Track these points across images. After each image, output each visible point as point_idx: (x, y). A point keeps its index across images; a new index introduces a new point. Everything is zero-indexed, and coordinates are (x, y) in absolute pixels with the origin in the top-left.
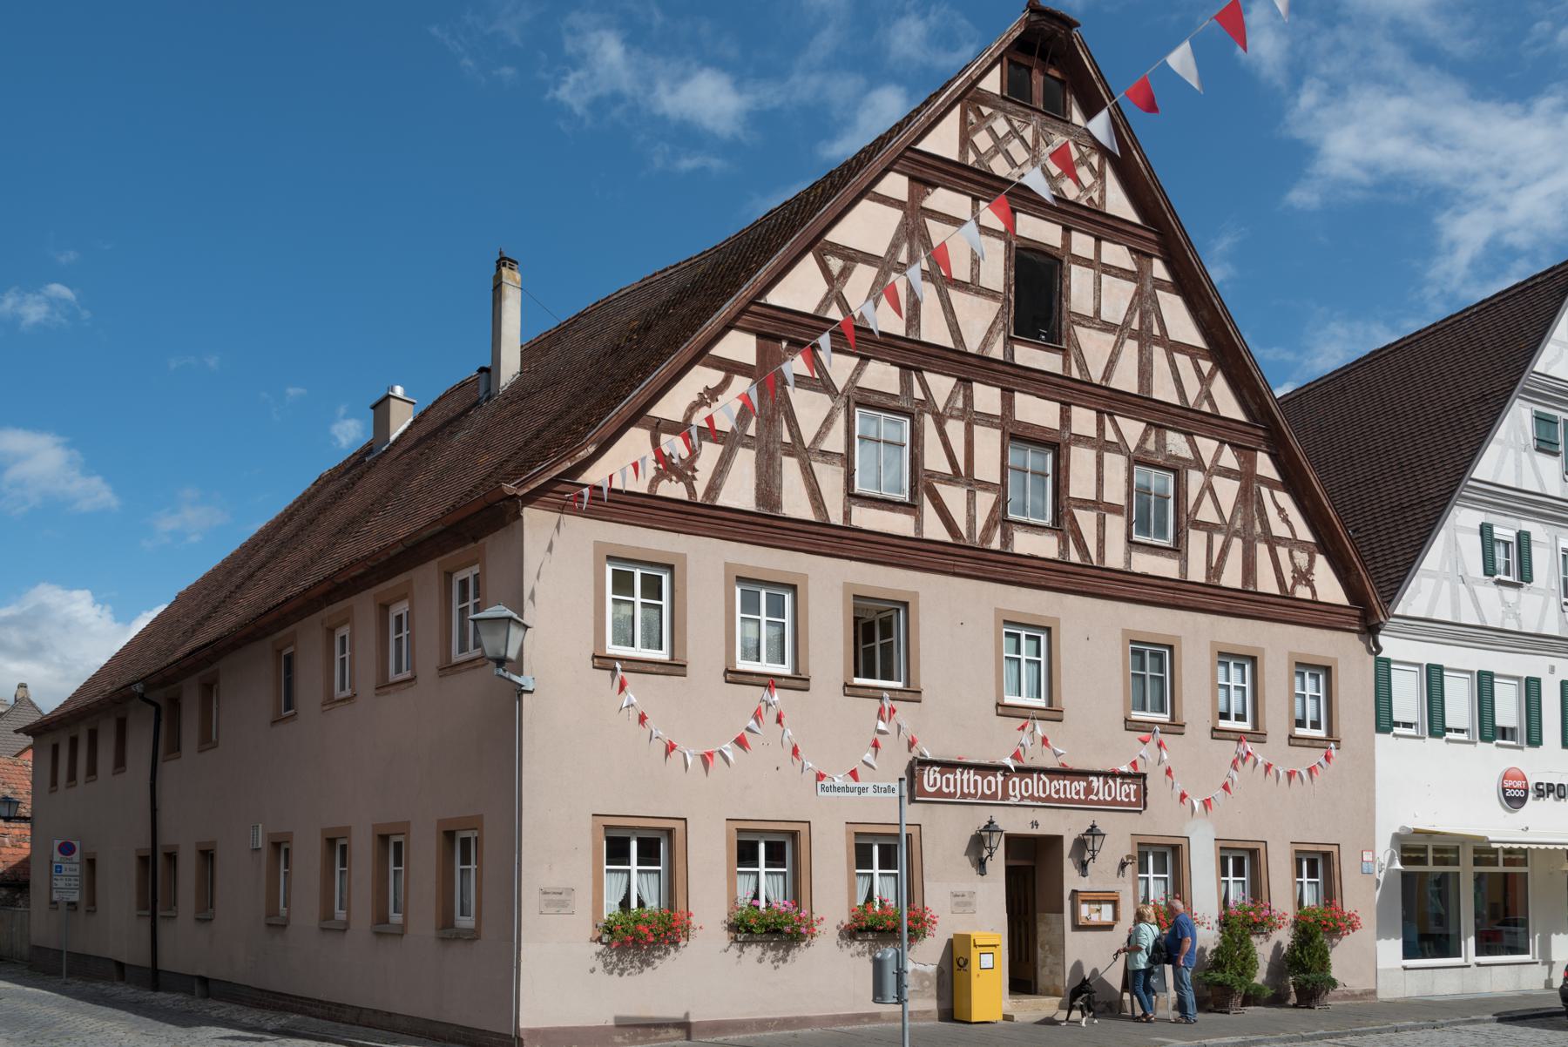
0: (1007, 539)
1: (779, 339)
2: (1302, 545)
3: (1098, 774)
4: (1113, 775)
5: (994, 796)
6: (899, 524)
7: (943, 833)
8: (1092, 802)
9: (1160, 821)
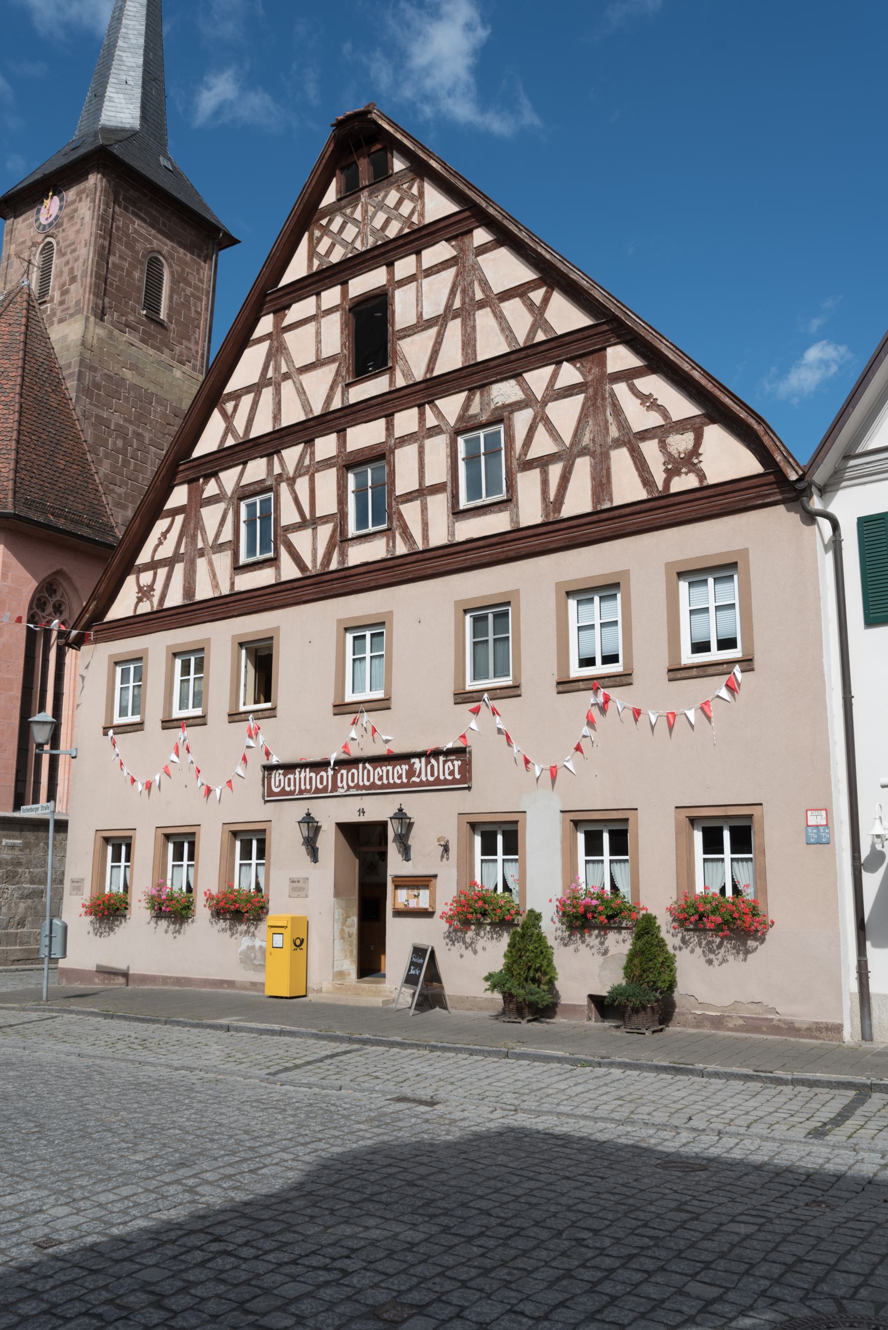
0: (343, 555)
1: (197, 479)
2: (681, 426)
3: (419, 755)
4: (436, 753)
5: (325, 789)
6: (264, 578)
7: (284, 826)
8: (415, 784)
9: (488, 798)
